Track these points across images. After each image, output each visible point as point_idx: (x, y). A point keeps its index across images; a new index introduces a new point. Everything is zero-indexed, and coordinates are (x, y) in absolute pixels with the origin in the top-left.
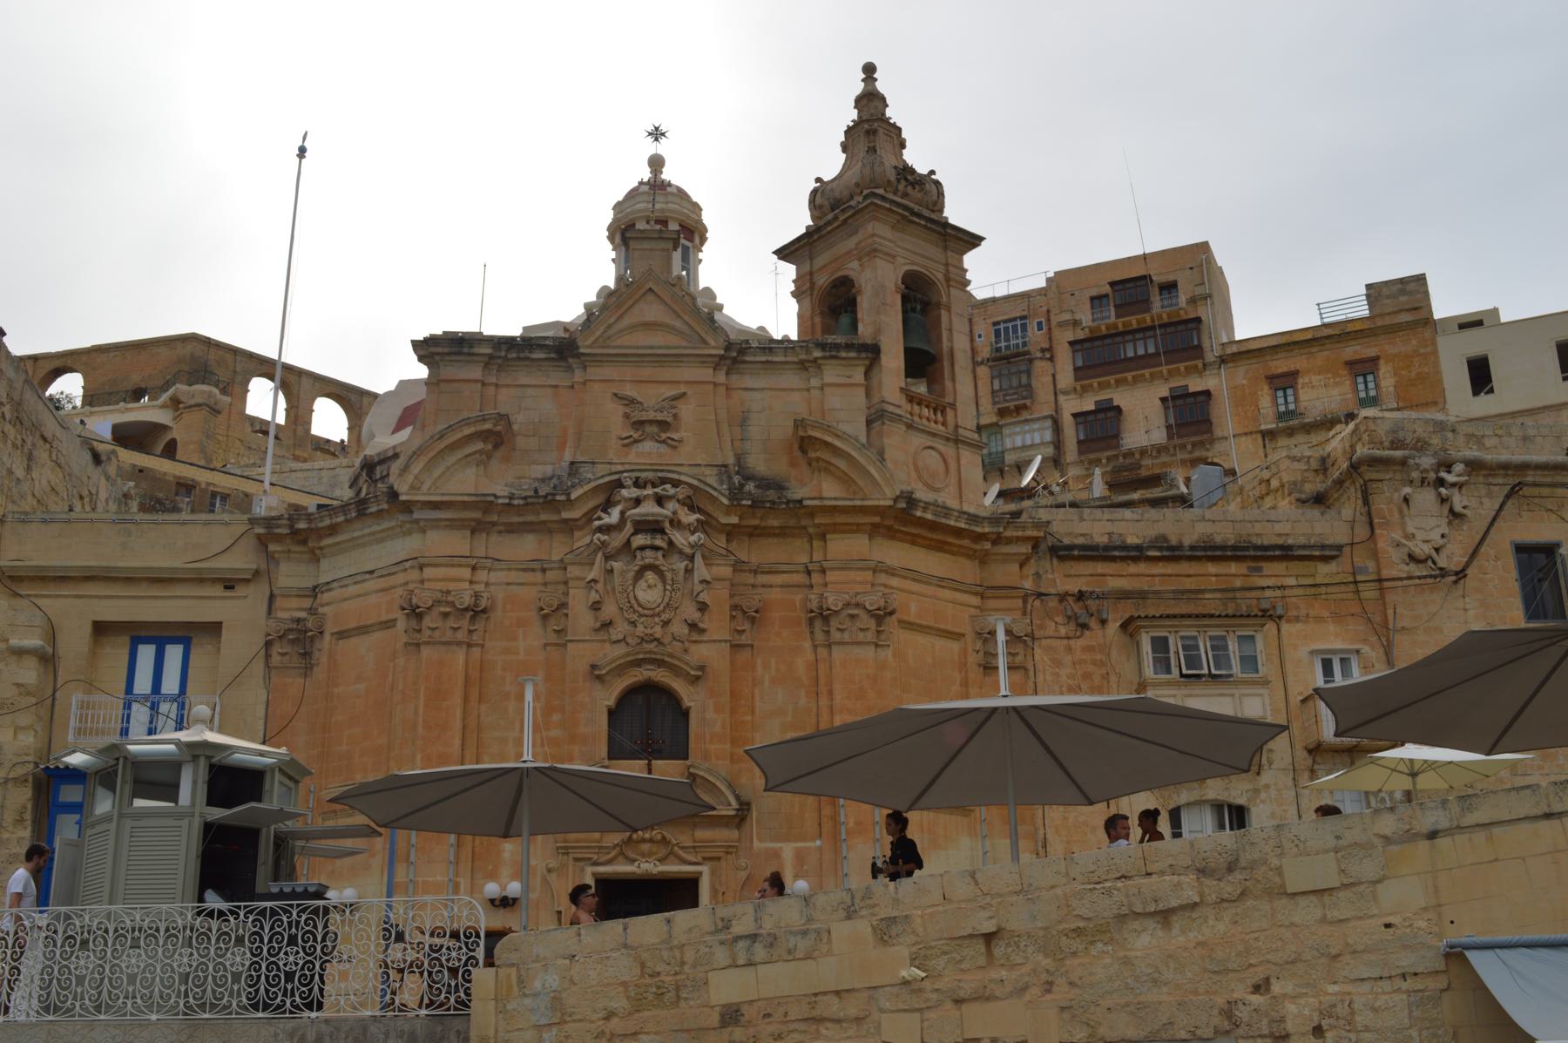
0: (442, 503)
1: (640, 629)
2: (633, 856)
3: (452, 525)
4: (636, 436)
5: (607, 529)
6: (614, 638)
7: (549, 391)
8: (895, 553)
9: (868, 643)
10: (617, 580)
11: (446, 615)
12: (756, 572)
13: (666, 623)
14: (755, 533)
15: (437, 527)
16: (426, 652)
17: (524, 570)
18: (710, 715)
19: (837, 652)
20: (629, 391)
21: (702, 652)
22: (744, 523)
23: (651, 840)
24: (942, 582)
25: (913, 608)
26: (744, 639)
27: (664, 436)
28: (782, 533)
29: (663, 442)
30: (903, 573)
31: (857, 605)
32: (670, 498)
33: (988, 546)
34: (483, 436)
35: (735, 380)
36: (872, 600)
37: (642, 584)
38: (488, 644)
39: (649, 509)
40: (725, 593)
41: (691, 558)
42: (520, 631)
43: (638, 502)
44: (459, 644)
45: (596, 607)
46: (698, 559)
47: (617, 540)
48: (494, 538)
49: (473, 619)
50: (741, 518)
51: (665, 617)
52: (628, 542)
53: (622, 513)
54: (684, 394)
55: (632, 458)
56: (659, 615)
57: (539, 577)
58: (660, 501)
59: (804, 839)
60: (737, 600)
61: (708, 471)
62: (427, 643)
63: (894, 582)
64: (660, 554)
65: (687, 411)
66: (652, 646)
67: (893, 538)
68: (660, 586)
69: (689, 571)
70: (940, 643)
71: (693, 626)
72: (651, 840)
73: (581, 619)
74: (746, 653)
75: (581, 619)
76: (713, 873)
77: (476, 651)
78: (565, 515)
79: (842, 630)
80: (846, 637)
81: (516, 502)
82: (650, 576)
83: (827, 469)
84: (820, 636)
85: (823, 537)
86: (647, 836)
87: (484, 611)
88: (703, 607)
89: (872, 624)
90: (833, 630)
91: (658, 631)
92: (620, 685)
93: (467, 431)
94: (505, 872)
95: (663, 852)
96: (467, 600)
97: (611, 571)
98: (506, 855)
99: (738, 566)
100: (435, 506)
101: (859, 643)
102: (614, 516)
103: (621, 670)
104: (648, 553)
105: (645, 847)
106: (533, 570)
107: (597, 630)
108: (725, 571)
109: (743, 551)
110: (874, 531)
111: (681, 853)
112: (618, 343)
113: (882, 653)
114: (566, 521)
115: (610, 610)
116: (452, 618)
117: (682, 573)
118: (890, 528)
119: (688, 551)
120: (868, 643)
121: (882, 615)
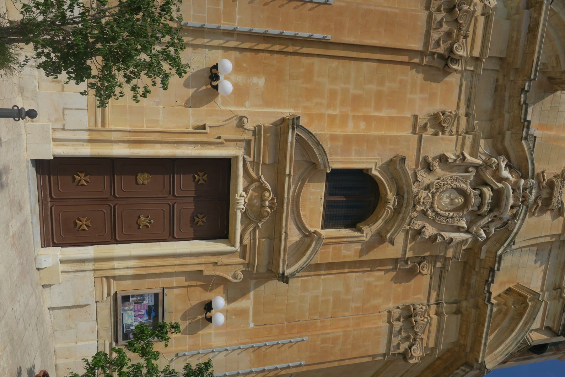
0: (535, 36)
6: (419, 174)
31: (415, 340)
41: (467, 232)
42: (426, 96)
44: (426, 44)
45: (443, 159)
47: (488, 176)
51: (430, 212)
52: (486, 184)
53: (507, 179)
56: (432, 207)
59: (255, 314)
64: (476, 209)
68: (450, 207)
69: (458, 229)
71: (419, 232)
78: (508, 134)
82: (460, 200)
85: (458, 312)
89: (401, 350)
91: (419, 208)
94: (240, 79)
95: (252, 216)
97: (467, 171)
98: (255, 80)
102: (505, 173)
107: (425, 159)
114: (502, 134)
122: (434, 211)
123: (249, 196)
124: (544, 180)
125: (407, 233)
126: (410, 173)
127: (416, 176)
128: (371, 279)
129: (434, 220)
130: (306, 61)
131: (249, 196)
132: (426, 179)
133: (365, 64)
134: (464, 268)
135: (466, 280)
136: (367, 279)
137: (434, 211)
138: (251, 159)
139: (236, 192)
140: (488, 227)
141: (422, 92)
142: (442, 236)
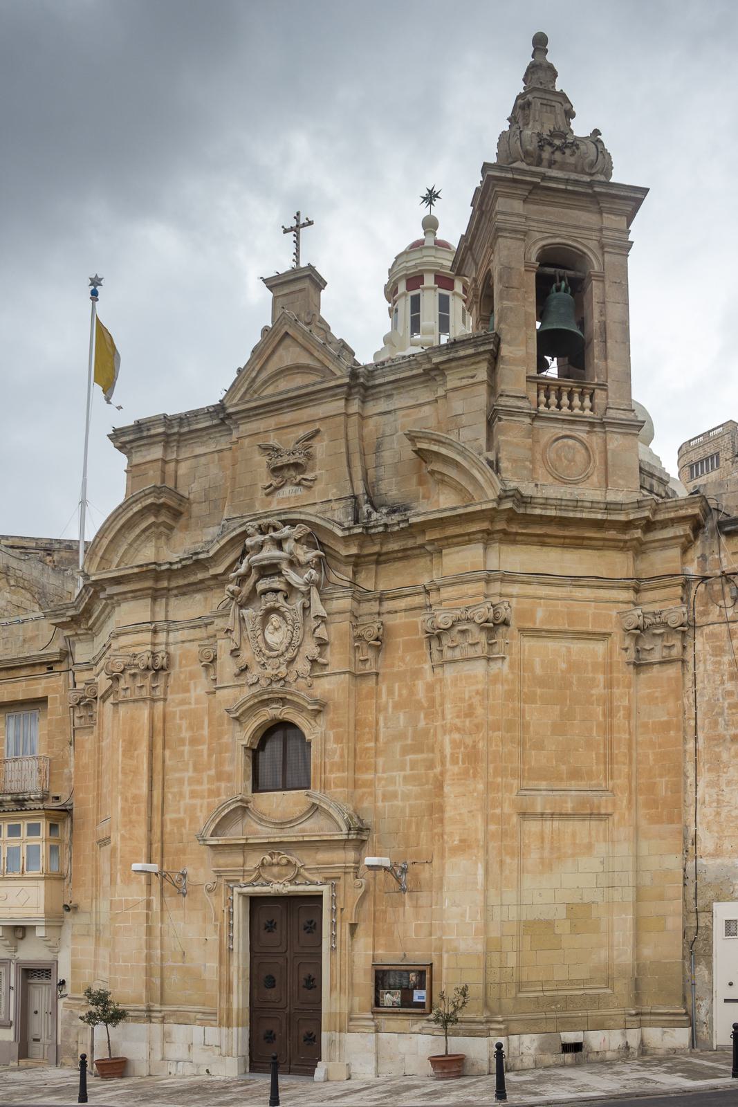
0: (122, 577)
1: (270, 671)
2: (269, 878)
3: (136, 595)
4: (275, 484)
5: (242, 579)
6: (250, 682)
7: (216, 456)
8: (515, 558)
9: (479, 658)
10: (249, 626)
11: (134, 675)
12: (381, 599)
13: (291, 661)
14: (380, 559)
15: (126, 600)
16: (122, 709)
17: (194, 627)
18: (331, 745)
19: (449, 672)
20: (273, 441)
21: (327, 686)
22: (366, 551)
23: (278, 864)
24: (576, 581)
25: (540, 614)
26: (369, 668)
27: (299, 478)
28: (405, 555)
29: (299, 484)
30: (525, 578)
32: (286, 539)
33: (638, 533)
34: (155, 509)
35: (375, 407)
36: (483, 612)
37: (270, 628)
38: (169, 697)
39: (269, 553)
40: (346, 625)
43: (260, 547)
44: (144, 700)
45: (235, 653)
46: (315, 594)
47: (246, 590)
48: (173, 602)
49: (155, 676)
50: (361, 546)
51: (288, 656)
52: (254, 589)
54: (318, 431)
55: (275, 506)
57: (199, 633)
58: (279, 544)
60: (359, 631)
61: (335, 505)
62: (123, 702)
63: (514, 589)
64: (280, 596)
65: (320, 448)
66: (276, 686)
67: (514, 542)
69: (306, 609)
70: (577, 646)
71: (314, 662)
72: (278, 864)
73: (227, 666)
74: (371, 682)
75: (227, 666)
76: (334, 887)
77: (160, 705)
78: (212, 572)
79: (453, 648)
80: (457, 654)
81: (175, 567)
82: (274, 618)
83: (442, 480)
84: (436, 655)
86: (275, 861)
87: (162, 668)
88: (322, 644)
89: (482, 638)
90: (445, 648)
92: (254, 723)
93: (136, 508)
95: (292, 874)
96: (145, 660)
99: (360, 596)
100: (118, 581)
101: (468, 659)
103: (251, 710)
104: (270, 596)
105: (275, 870)
106: (200, 627)
107: (237, 675)
108: (345, 603)
109: (366, 582)
110: (488, 537)
111: (306, 874)
112: (265, 394)
113: (495, 667)
114: (215, 577)
115: (246, 655)
116: (139, 678)
117: (300, 612)
118: (504, 532)
119: (303, 589)
120: (479, 658)
121: (495, 625)
122: (287, 650)
123: (273, 879)
124: (271, 485)
125: (318, 677)
126: (255, 689)
127: (253, 684)
128: (390, 705)
129: (299, 646)
130: (168, 828)
131: (273, 879)
132: (255, 673)
133: (168, 762)
134: (385, 562)
135: (400, 555)
136: (390, 710)
137: (287, 650)
138: (241, 878)
139: (270, 892)
140: (308, 562)
141: (188, 691)
142: (315, 630)
